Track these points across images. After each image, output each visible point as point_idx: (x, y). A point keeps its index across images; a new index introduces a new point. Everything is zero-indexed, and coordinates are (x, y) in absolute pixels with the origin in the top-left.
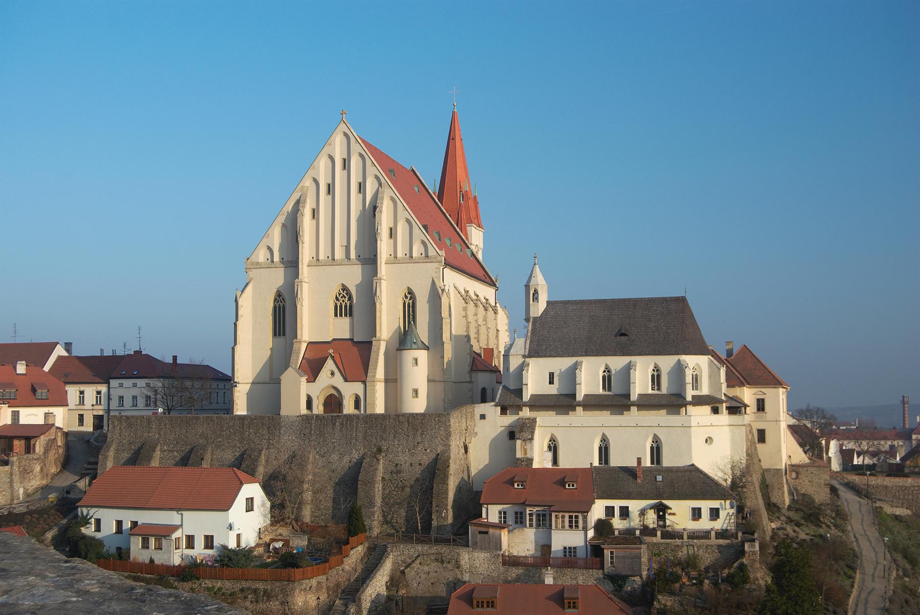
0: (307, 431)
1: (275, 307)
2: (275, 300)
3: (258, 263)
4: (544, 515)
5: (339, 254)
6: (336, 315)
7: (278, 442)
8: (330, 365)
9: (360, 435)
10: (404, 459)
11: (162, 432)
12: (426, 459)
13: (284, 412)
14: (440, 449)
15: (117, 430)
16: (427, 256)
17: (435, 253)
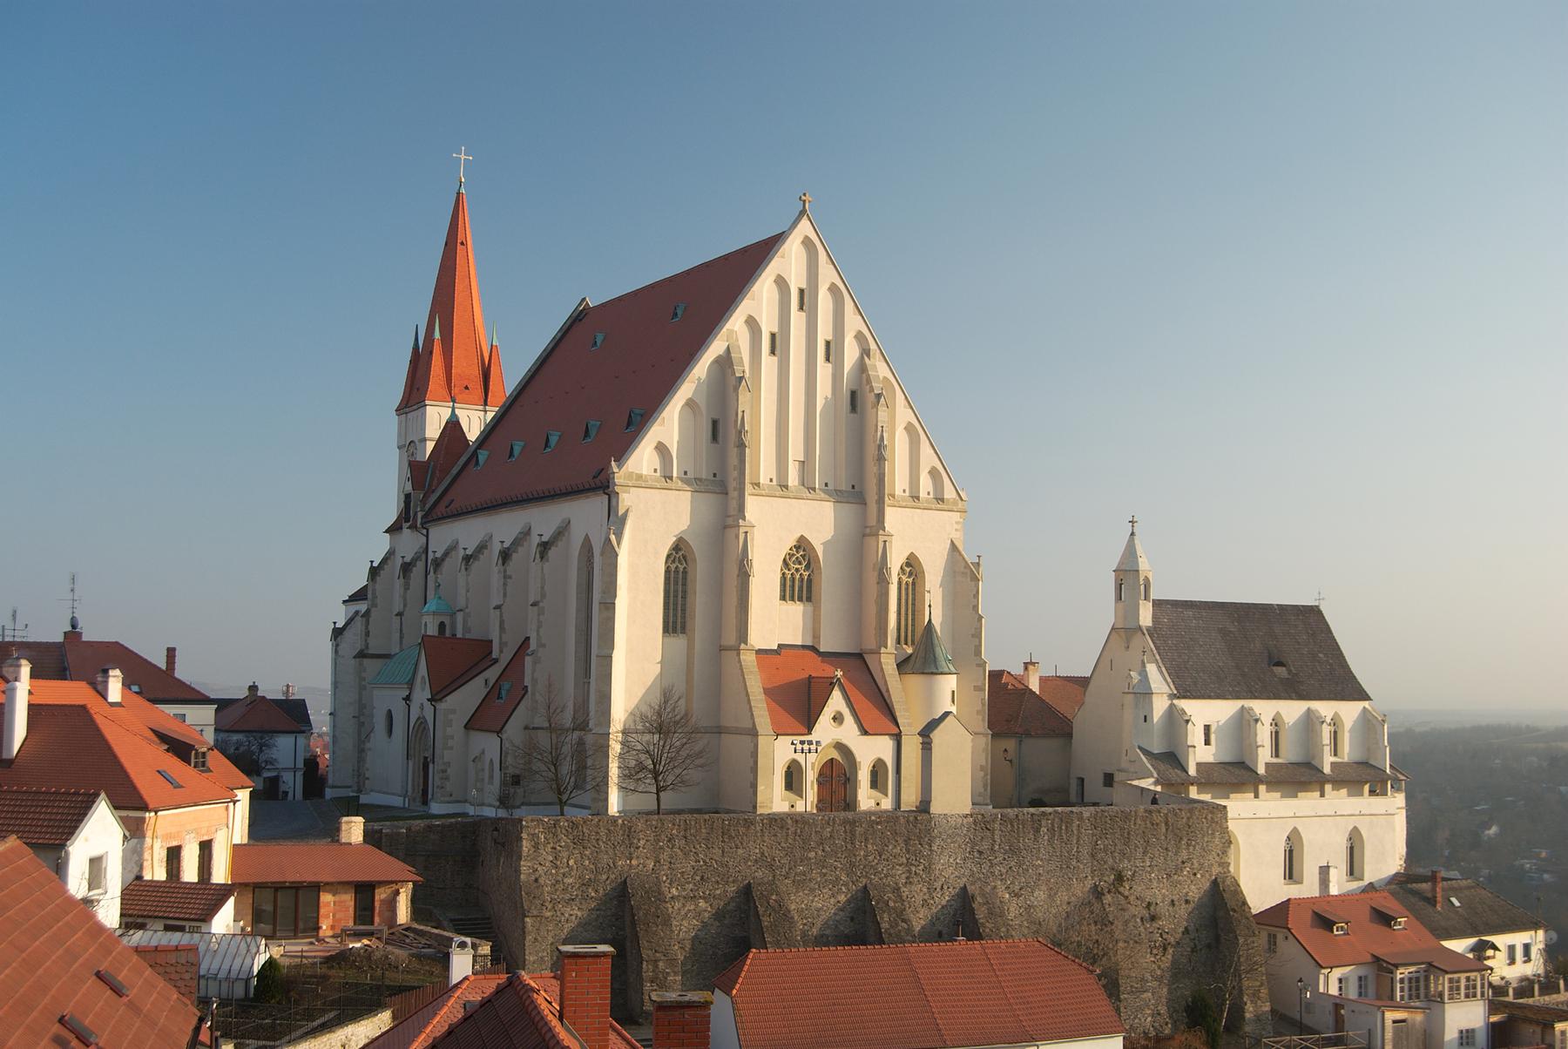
0: (985, 846)
1: (667, 571)
2: (668, 556)
3: (640, 477)
4: (1417, 979)
5: (793, 479)
6: (783, 598)
7: (928, 869)
8: (836, 702)
9: (1085, 851)
10: (1160, 893)
11: (664, 856)
12: (1196, 889)
13: (936, 808)
14: (1216, 870)
15: (546, 855)
16: (940, 499)
17: (954, 495)
